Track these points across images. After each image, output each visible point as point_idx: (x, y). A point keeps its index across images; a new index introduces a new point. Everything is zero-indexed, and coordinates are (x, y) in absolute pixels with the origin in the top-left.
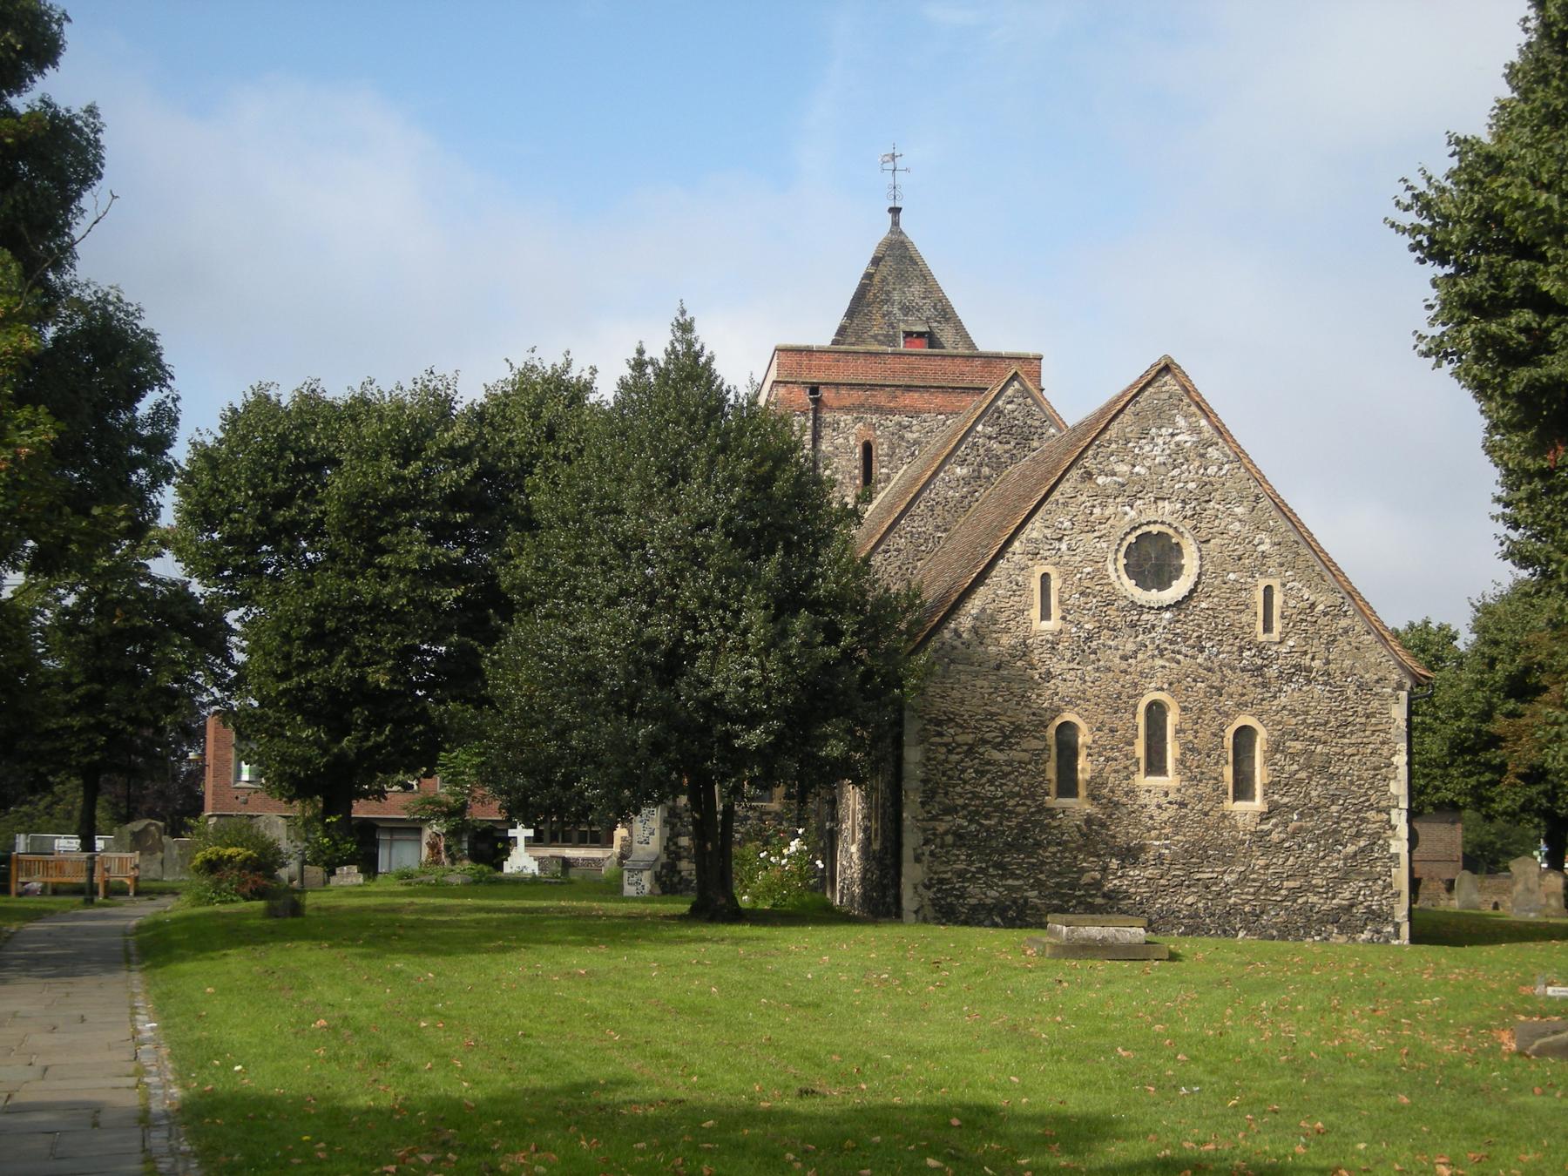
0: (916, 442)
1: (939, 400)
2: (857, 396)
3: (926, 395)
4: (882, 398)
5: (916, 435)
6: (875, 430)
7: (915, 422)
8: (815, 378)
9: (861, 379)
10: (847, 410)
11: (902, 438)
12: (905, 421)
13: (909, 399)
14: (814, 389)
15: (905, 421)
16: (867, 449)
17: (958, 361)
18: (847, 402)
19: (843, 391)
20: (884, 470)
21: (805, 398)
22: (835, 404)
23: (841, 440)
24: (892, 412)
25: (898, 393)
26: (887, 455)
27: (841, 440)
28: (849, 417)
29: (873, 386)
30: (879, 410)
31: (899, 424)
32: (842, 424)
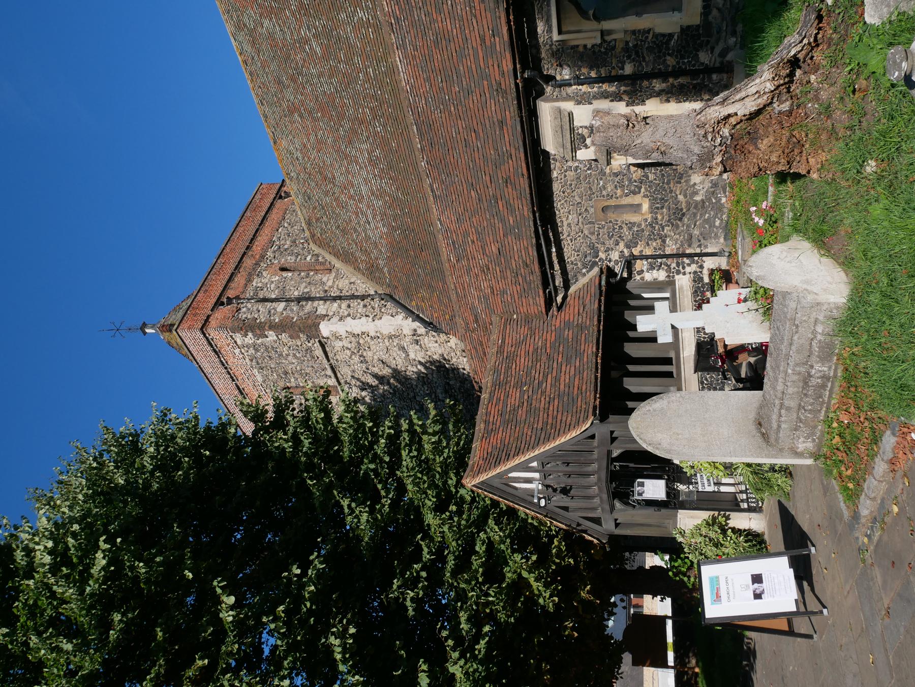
0: (294, 242)
1: (266, 231)
2: (240, 279)
3: (259, 238)
4: (248, 262)
5: (288, 242)
6: (273, 264)
7: (278, 243)
8: (214, 300)
9: (227, 277)
10: (249, 280)
11: (286, 250)
12: (275, 248)
13: (257, 248)
14: (222, 304)
15: (275, 248)
16: (283, 269)
17: (242, 223)
18: (243, 282)
19: (232, 285)
20: (308, 258)
21: (224, 311)
22: (241, 289)
23: (273, 286)
24: (262, 257)
25: (250, 253)
26: (297, 257)
27: (273, 286)
28: (255, 280)
29: (237, 267)
30: (257, 264)
31: (274, 252)
32: (260, 285)
